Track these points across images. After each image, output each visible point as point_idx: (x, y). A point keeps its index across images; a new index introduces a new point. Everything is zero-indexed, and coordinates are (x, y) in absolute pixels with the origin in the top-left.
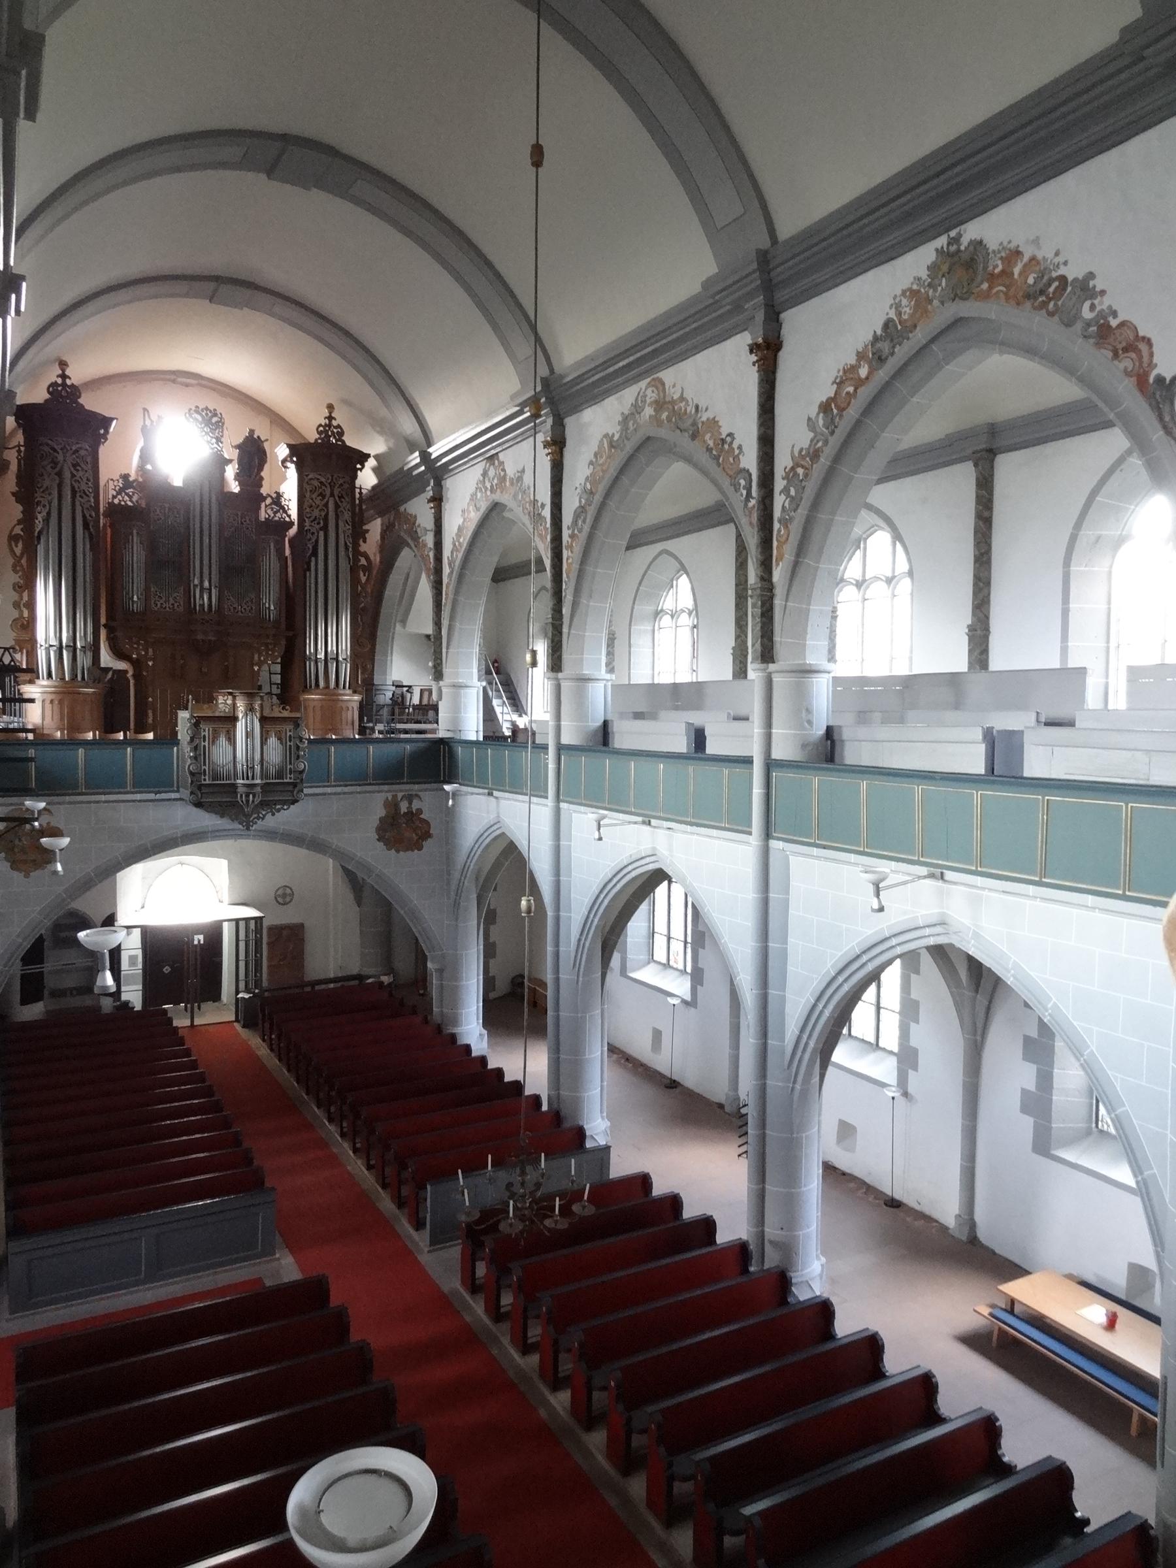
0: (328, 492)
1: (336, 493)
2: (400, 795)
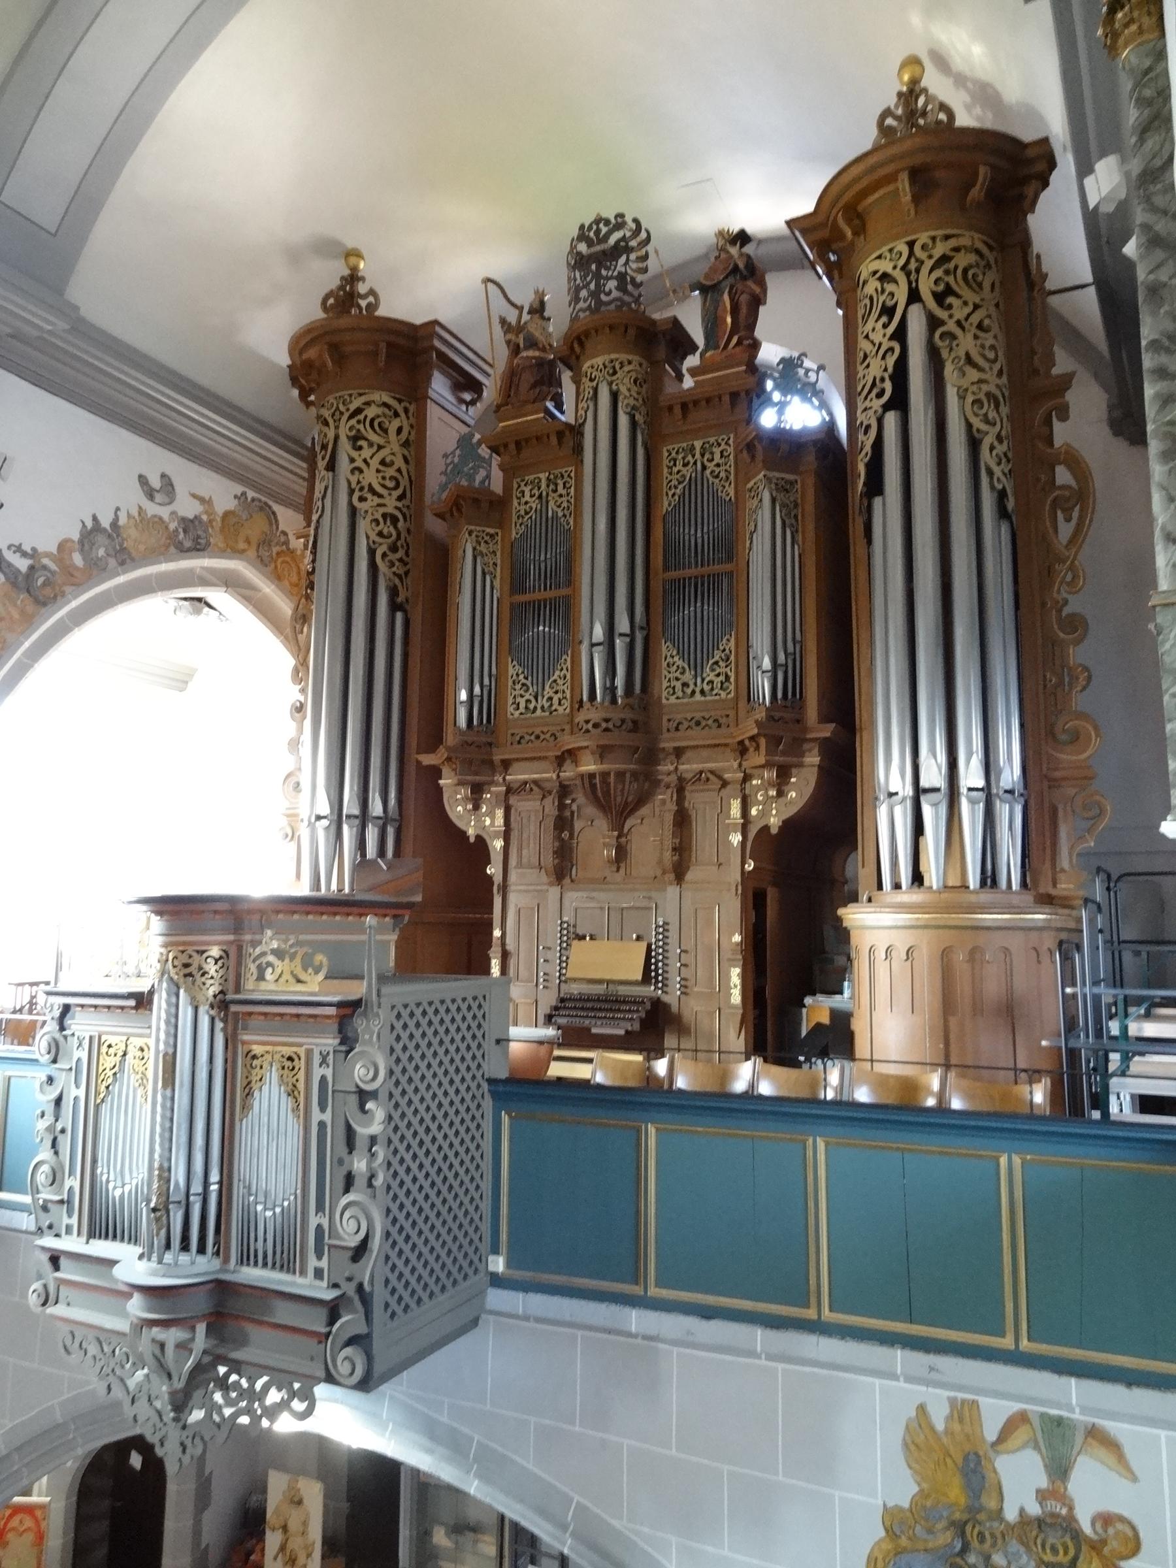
0: (902, 295)
1: (926, 287)
2: (994, 1415)
